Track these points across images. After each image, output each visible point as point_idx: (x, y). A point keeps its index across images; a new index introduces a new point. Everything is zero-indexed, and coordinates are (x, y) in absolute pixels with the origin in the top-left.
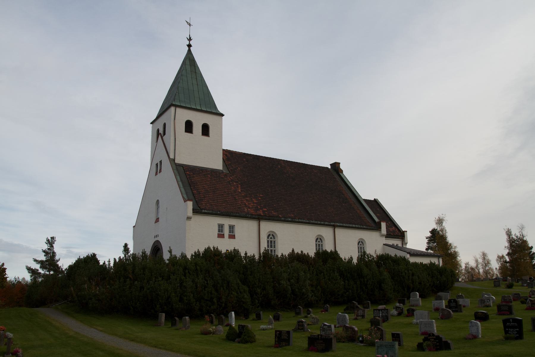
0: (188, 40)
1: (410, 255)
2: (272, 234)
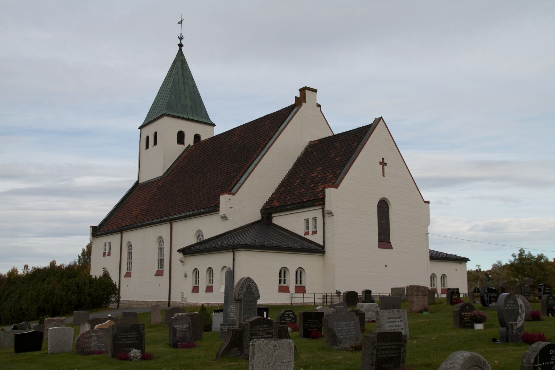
0: (179, 38)
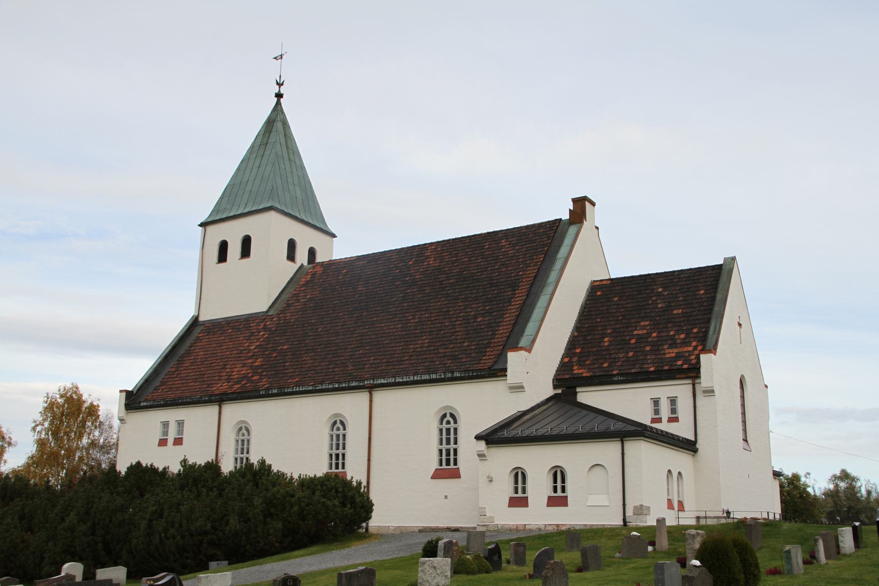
0: (278, 84)
1: (487, 444)
2: (245, 427)
